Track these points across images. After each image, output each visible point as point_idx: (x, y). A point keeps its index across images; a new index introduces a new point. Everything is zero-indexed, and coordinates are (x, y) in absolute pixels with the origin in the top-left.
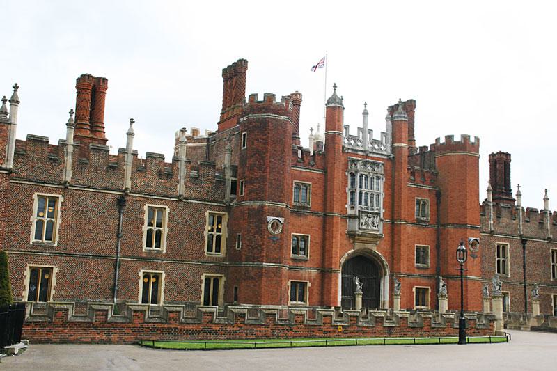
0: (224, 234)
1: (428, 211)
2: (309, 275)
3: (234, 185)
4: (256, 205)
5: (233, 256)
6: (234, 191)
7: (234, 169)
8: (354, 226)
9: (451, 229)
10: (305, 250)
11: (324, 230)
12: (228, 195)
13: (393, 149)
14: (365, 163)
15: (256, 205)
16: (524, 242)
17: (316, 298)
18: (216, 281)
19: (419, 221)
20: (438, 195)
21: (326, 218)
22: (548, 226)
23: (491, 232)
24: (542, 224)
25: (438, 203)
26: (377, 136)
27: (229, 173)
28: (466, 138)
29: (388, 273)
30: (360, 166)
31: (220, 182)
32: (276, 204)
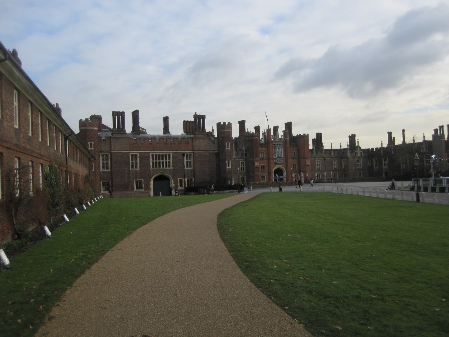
0: (245, 166)
1: (296, 154)
2: (266, 174)
3: (246, 154)
4: (252, 159)
5: (248, 172)
6: (246, 155)
7: (246, 150)
8: (275, 161)
9: (301, 159)
10: (264, 168)
11: (268, 162)
12: (245, 157)
13: (285, 140)
14: (278, 145)
15: (252, 159)
16: (325, 159)
17: (268, 180)
18: (244, 177)
19: (293, 158)
20: (298, 150)
21: (269, 159)
22: (332, 154)
23: (315, 158)
24: (330, 153)
25: (298, 152)
26: (280, 137)
27: (244, 152)
28: (304, 134)
29: (285, 172)
30: (276, 146)
31: (243, 154)
32: (256, 159)
